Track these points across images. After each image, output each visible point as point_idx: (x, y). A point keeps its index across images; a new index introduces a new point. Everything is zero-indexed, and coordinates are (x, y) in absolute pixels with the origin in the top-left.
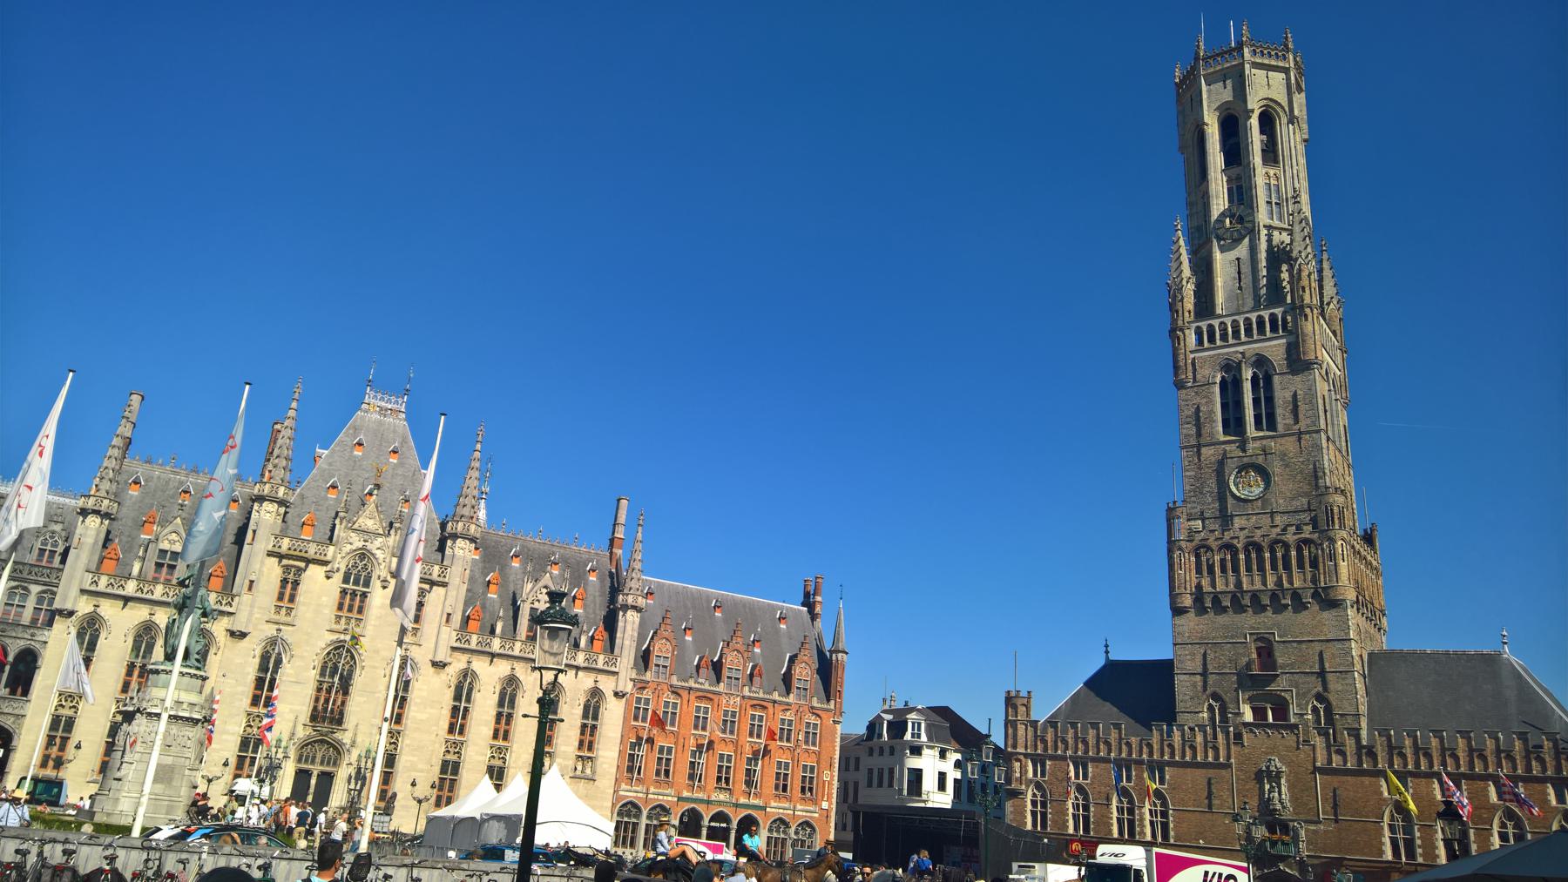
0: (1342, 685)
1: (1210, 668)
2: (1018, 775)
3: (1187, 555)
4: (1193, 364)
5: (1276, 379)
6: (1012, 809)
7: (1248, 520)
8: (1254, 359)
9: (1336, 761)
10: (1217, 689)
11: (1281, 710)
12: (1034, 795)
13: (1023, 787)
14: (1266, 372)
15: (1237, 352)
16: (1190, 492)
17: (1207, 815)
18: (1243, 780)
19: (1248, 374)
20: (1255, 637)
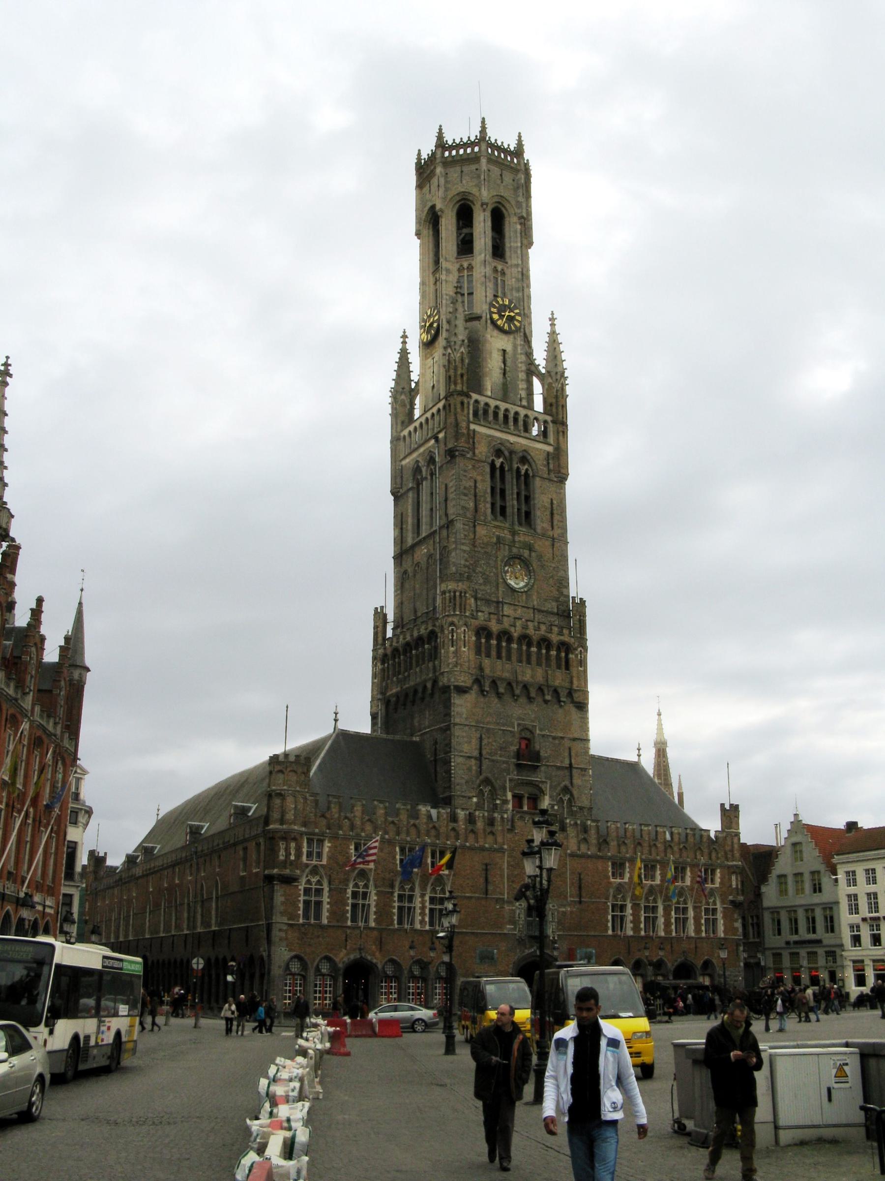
0: (582, 780)
1: (484, 752)
2: (292, 858)
3: (470, 633)
4: (474, 438)
5: (538, 482)
6: (282, 899)
7: (515, 610)
8: (521, 454)
9: (584, 848)
10: (489, 775)
11: (534, 800)
12: (309, 882)
13: (298, 872)
14: (527, 470)
15: (508, 441)
16: (465, 566)
17: (483, 902)
18: (512, 866)
19: (515, 466)
20: (521, 728)
